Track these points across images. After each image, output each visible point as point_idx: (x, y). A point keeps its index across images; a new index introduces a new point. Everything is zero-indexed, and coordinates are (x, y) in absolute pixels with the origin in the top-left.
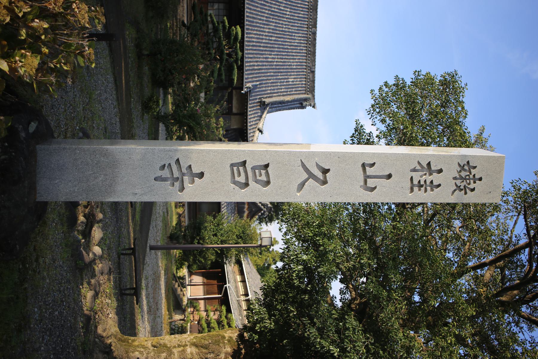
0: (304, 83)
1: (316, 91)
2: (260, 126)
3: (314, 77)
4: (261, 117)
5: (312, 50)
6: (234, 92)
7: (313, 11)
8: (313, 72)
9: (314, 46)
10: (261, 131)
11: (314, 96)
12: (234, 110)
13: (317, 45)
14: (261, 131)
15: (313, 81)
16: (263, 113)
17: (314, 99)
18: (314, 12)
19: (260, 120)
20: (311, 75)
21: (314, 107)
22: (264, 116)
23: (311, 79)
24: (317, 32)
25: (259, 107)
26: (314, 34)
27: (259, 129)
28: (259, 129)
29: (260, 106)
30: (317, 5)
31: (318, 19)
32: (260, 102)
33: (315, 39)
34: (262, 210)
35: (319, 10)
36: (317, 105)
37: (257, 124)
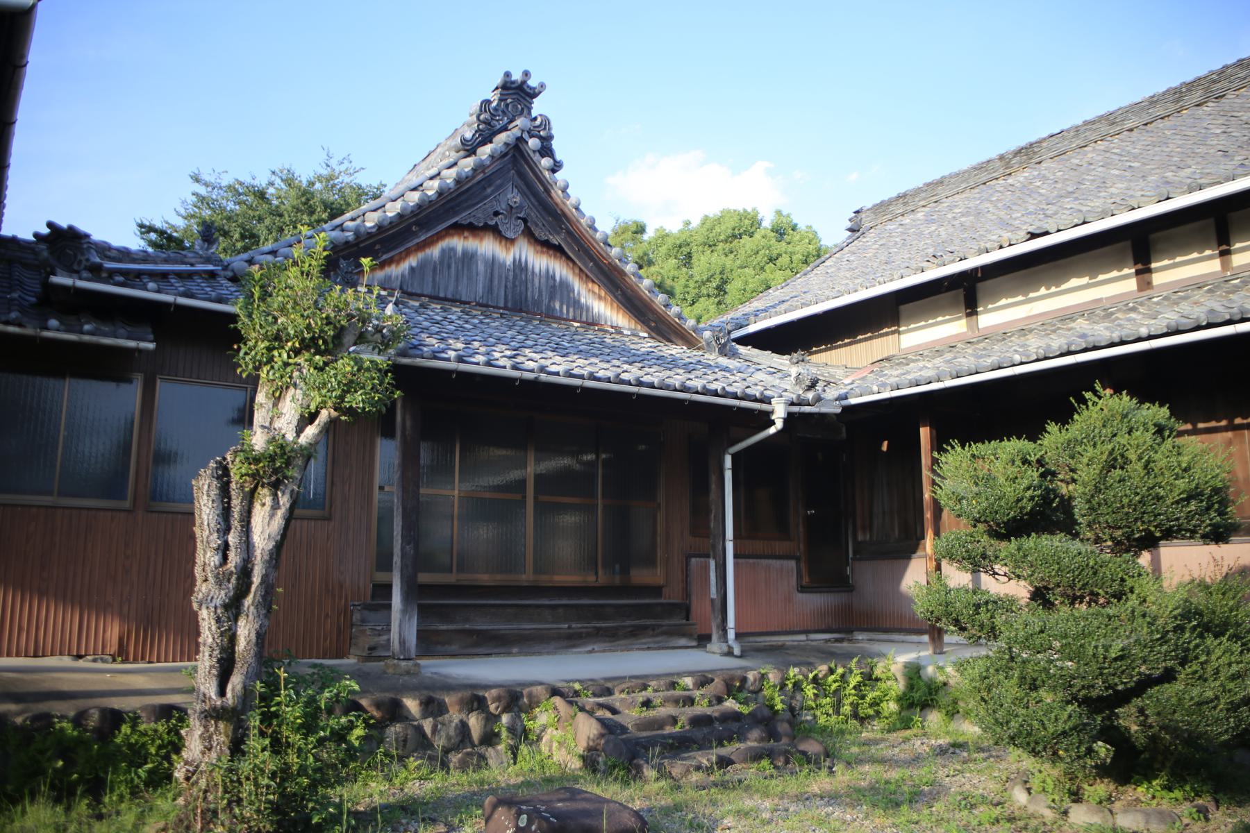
34: (520, 139)
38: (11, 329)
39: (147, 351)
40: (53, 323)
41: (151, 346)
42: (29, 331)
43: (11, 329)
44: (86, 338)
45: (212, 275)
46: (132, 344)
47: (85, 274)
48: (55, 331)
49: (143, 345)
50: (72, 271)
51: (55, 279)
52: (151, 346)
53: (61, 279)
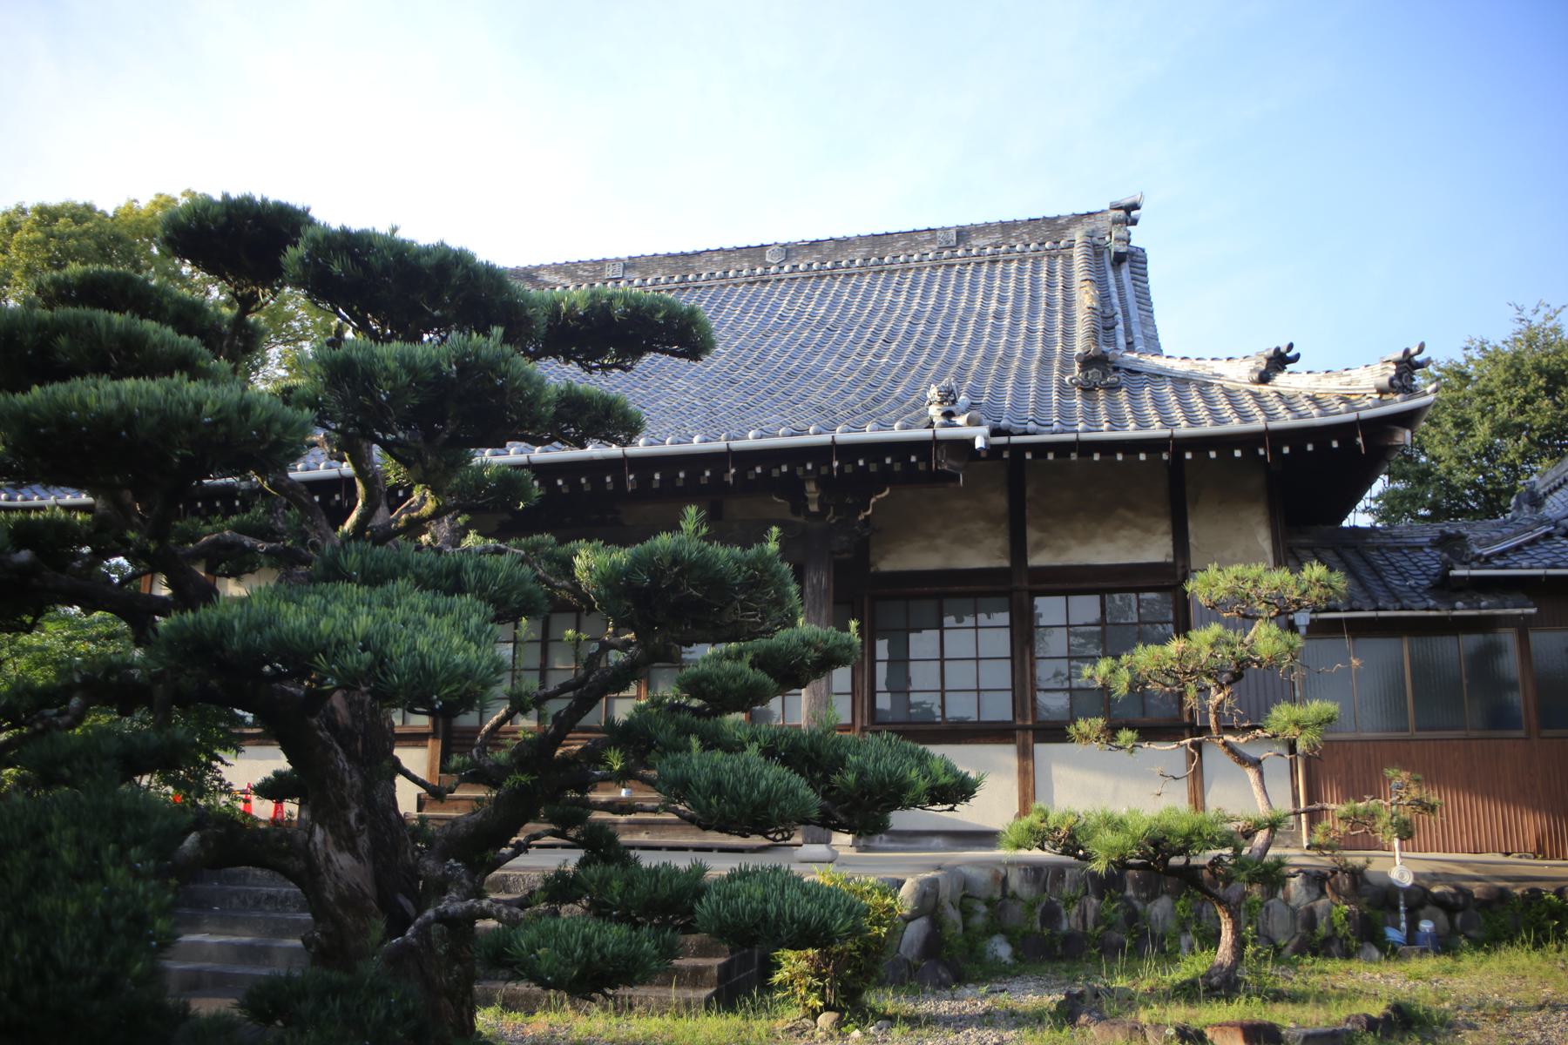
0: (1014, 265)
1: (1051, 214)
2: (1239, 374)
3: (985, 229)
4: (1181, 382)
5: (863, 251)
6: (1037, 560)
7: (693, 269)
8: (963, 234)
9: (841, 244)
10: (1280, 361)
11: (1078, 218)
12: (1157, 550)
13: (838, 234)
14: (1280, 361)
15: (1006, 227)
16: (1158, 376)
17: (1089, 214)
18: (697, 263)
19: (1204, 386)
20: (977, 242)
21: (1128, 212)
22: (1181, 367)
23: (997, 237)
24: (783, 240)
25: (1122, 395)
26: (789, 250)
27: (1264, 378)
28: (1264, 378)
29: (1112, 388)
30: (669, 256)
31: (727, 246)
32: (1088, 390)
33: (815, 244)
35: (689, 249)
36: (1125, 198)
37: (1229, 394)
38: (1432, 613)
39: (1530, 615)
40: (1459, 604)
41: (1533, 611)
42: (1443, 613)
43: (1432, 613)
44: (1484, 612)
45: (1548, 536)
46: (1518, 611)
47: (1475, 564)
48: (1461, 610)
49: (1527, 611)
50: (1465, 564)
51: (1453, 573)
52: (1533, 611)
53: (1459, 572)
